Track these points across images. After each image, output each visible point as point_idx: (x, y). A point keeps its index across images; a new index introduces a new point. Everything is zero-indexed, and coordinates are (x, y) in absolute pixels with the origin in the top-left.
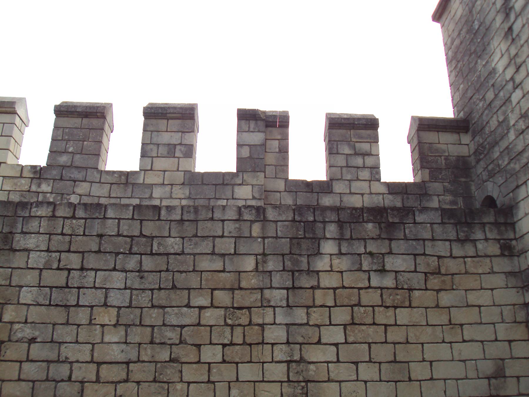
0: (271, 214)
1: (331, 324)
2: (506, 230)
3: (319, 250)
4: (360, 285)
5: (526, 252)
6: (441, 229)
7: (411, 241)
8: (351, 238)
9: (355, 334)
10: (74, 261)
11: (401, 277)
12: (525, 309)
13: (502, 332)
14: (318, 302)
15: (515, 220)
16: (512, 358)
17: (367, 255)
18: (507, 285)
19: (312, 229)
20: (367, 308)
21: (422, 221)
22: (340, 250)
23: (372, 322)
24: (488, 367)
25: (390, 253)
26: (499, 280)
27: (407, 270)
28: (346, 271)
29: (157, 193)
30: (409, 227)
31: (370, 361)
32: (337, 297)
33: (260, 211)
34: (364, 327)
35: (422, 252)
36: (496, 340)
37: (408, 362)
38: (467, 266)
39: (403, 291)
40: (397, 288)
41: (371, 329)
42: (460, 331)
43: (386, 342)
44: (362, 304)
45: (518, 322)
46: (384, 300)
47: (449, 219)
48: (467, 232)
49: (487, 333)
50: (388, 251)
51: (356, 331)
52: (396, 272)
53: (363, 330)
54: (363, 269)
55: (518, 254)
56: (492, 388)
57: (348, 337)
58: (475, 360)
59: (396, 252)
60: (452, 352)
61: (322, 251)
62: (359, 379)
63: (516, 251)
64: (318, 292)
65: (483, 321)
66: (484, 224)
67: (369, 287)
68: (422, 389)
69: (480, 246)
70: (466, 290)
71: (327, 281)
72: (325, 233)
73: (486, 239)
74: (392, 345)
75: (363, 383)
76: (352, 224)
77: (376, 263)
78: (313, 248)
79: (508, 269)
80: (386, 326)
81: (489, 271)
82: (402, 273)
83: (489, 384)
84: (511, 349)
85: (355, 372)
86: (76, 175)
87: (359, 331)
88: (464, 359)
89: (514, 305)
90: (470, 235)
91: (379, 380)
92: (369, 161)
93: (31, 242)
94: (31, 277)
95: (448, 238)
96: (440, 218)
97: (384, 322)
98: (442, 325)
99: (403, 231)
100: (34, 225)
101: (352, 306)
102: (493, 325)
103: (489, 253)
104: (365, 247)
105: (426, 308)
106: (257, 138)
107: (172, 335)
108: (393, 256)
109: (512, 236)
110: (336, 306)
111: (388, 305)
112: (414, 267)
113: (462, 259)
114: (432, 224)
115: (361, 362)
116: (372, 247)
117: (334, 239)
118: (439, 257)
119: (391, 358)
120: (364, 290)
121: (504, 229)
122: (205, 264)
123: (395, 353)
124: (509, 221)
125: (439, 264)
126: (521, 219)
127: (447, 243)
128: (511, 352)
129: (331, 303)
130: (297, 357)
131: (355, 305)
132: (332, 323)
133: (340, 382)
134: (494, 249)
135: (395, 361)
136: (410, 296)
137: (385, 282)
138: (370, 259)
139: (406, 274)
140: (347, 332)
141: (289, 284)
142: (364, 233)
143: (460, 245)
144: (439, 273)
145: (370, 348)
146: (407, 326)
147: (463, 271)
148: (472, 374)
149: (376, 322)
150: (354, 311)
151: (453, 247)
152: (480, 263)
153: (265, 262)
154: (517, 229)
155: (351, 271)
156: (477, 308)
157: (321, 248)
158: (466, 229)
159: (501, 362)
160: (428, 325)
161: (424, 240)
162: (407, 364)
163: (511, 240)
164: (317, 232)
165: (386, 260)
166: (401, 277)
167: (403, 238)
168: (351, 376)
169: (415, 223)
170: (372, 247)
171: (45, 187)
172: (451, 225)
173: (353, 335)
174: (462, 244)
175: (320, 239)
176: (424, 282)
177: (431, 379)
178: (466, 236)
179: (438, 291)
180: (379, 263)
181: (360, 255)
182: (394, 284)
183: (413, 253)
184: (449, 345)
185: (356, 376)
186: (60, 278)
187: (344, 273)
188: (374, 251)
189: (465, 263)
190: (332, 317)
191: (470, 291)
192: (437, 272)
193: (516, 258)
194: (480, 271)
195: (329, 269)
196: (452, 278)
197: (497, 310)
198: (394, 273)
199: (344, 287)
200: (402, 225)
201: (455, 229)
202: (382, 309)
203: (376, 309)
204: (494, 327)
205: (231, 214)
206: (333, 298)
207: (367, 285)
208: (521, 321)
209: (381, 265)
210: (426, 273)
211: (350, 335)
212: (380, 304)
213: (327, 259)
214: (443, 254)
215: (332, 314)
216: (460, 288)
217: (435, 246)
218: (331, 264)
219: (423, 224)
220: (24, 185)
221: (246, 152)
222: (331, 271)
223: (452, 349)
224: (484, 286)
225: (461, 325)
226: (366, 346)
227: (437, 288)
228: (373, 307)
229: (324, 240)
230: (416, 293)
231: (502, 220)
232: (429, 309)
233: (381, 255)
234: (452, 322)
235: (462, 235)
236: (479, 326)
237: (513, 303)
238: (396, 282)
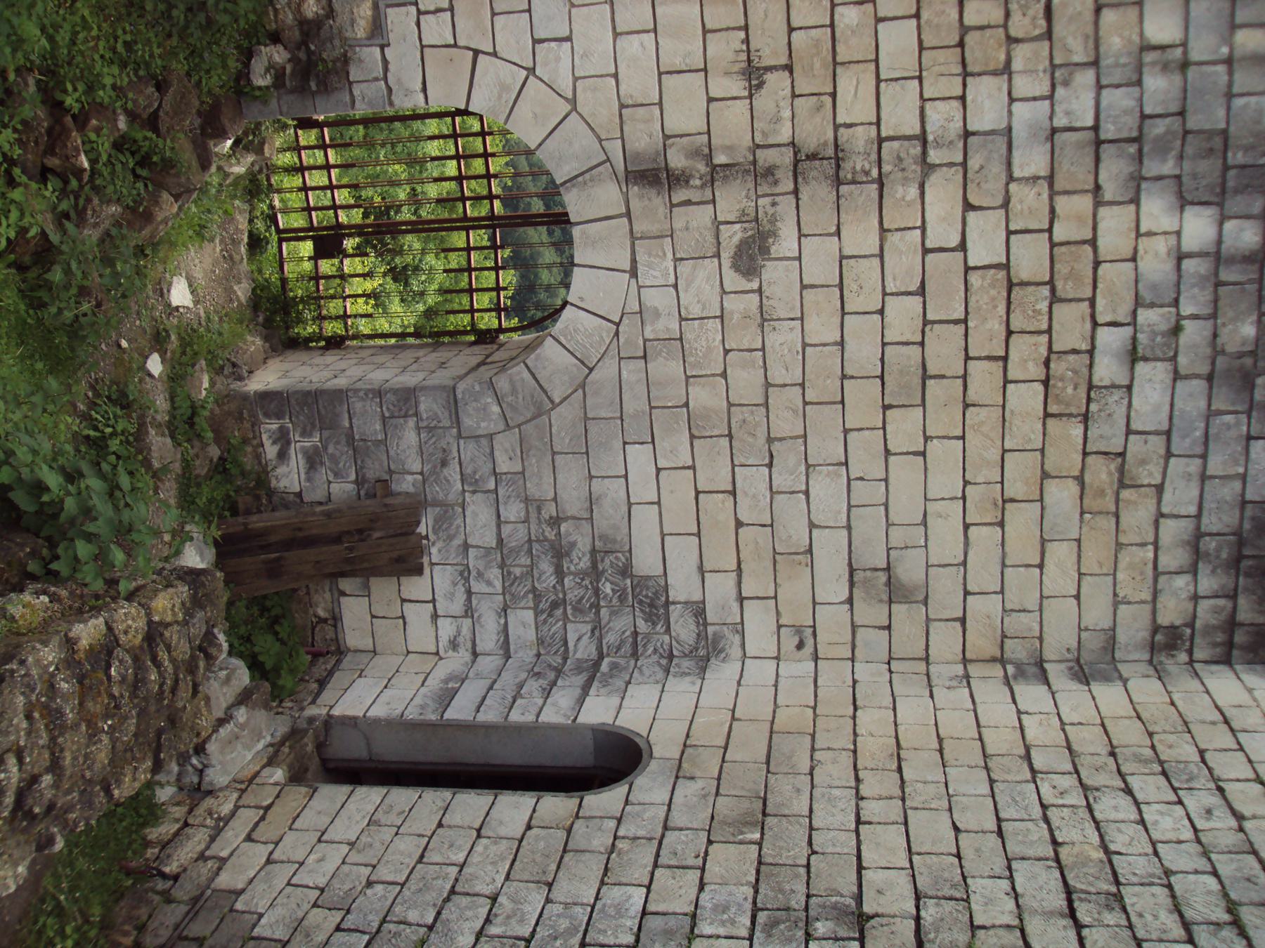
1: (1009, 233)
2: (1215, 645)
3: (1192, 203)
4: (1100, 303)
5: (1160, 678)
6: (1228, 498)
7: (1202, 425)
8: (1218, 284)
9: (987, 290)
11: (1116, 398)
12: (1032, 661)
13: (984, 609)
14: (1062, 203)
15: (1238, 667)
16: (928, 619)
17: (1173, 320)
18: (1087, 629)
19: (1247, 186)
20: (1046, 317)
21: (1253, 455)
22: (1190, 255)
23: (1012, 328)
24: (910, 570)
25: (1177, 376)
26: (1097, 613)
27: (1132, 414)
28: (1136, 269)
30: (1238, 424)
31: (926, 323)
32: (1073, 248)
34: (1002, 309)
35: (1174, 450)
36: (967, 593)
37: (923, 404)
38: (1134, 548)
39: (1084, 401)
40: (1091, 387)
41: (997, 326)
42: (988, 521)
43: (968, 358)
44: (1055, 306)
45: (1002, 642)
46: (1064, 357)
47: (1253, 519)
48: (1218, 557)
49: (983, 574)
50: (1182, 371)
51: (993, 292)
52: (1129, 388)
53: (995, 307)
54: (1140, 311)
55: (1155, 662)
56: (868, 573)
57: (980, 272)
58: (926, 546)
59: (1177, 391)
60: (943, 499)
61: (1190, 212)
62: (887, 298)
63: (1163, 659)
64: (1086, 202)
65: (1008, 571)
66: (1233, 596)
67: (1095, 324)
68: (867, 433)
69: (1181, 582)
70: (1079, 541)
71: (1114, 224)
72: (1236, 217)
73: (1195, 598)
74: (961, 372)
75: (879, 307)
76: (1256, 286)
77: (1153, 340)
78: (1197, 189)
79: (1122, 637)
80: (1005, 359)
81: (1121, 595)
82: (1125, 402)
83: (876, 570)
84: (947, 620)
85: (903, 290)
87: (993, 299)
88: (929, 525)
89: (1041, 639)
90: (1210, 562)
91: (886, 340)
95: (1205, 513)
96: (1258, 499)
97: (1014, 356)
98: (1002, 483)
99: (1231, 408)
101: (1051, 283)
102: (998, 589)
103: (1161, 599)
104: (1195, 317)
105: (1042, 451)
108: (1169, 382)
109: (1198, 654)
110: (1053, 245)
111: (1052, 365)
112: (1140, 429)
113: (1151, 539)
114: (1243, 478)
115: (924, 303)
116: (1193, 333)
117: (1219, 242)
118: (1160, 489)
119: (932, 370)
120: (1088, 311)
121: (1218, 640)
123: (943, 377)
124: (1235, 653)
125: (1143, 486)
126: (1239, 678)
127: (1193, 510)
128: (940, 620)
129: (1060, 233)
130: (934, 156)
131: (1053, 291)
132: (1013, 237)
133: (881, 256)
134: (1171, 612)
135: (925, 377)
136: (1070, 415)
137: (1106, 360)
138: (1164, 327)
139: (1124, 409)
140: (992, 271)
141: (1108, 131)
142: (1230, 314)
143: (1186, 537)
144: (1122, 485)
145: (956, 322)
146: (1004, 407)
147: (1122, 539)
148: (897, 536)
149: (1014, 338)
150: (1040, 288)
151: (1183, 523)
152: (1138, 578)
153: (1165, 67)
154: (1214, 668)
155: (1137, 282)
156: (1037, 561)
157: (1197, 208)
158: (1224, 555)
159: (921, 597)
160: (1004, 451)
161: (1204, 457)
162: (919, 402)
163: (1190, 652)
164: (1239, 198)
165: (1159, 364)
166: (1116, 398)
167: (1213, 408)
168: (894, 279)
169: (1249, 438)
170: (1193, 333)
172: (1236, 521)
173: (986, 285)
174: (1188, 543)
175: (1220, 205)
176: (1103, 450)
177: (887, 452)
178: (1207, 554)
179: (1080, 480)
180: (1153, 349)
181: (1176, 303)
182: (1101, 380)
183: (1174, 429)
184: (960, 495)
185: (894, 290)
187: (1130, 265)
188: (1184, 339)
189: (1143, 545)
190: (1027, 236)
191: (1076, 549)
193: (1147, 656)
194: (1120, 576)
195: (1143, 229)
196: (1108, 513)
197: (1032, 602)
198: (1126, 382)
199: (1097, 264)
200: (1244, 407)
201: (1226, 530)
202: (1043, 351)
203: (1044, 339)
204: (995, 593)
206: (1073, 239)
207: (1100, 320)
208: (1006, 647)
209: (1148, 354)
210: (1122, 455)
211: (983, 278)
212: (1056, 348)
213: (1167, 222)
214: (1167, 496)
215: (1035, 235)
216: (1085, 529)
217: (1189, 480)
218: (1156, 234)
219: (1243, 458)
222: (1138, 235)
223: (951, 499)
224: (1087, 581)
225: (1001, 524)
226: (960, 314)
227: (1087, 478)
228: (1049, 331)
229: (1218, 217)
230: (1078, 431)
231: (1239, 637)
232: (1039, 457)
233: (1172, 354)
234: (1008, 505)
235: (1210, 544)
236: (999, 561)
237: (1045, 636)
238: (1105, 387)
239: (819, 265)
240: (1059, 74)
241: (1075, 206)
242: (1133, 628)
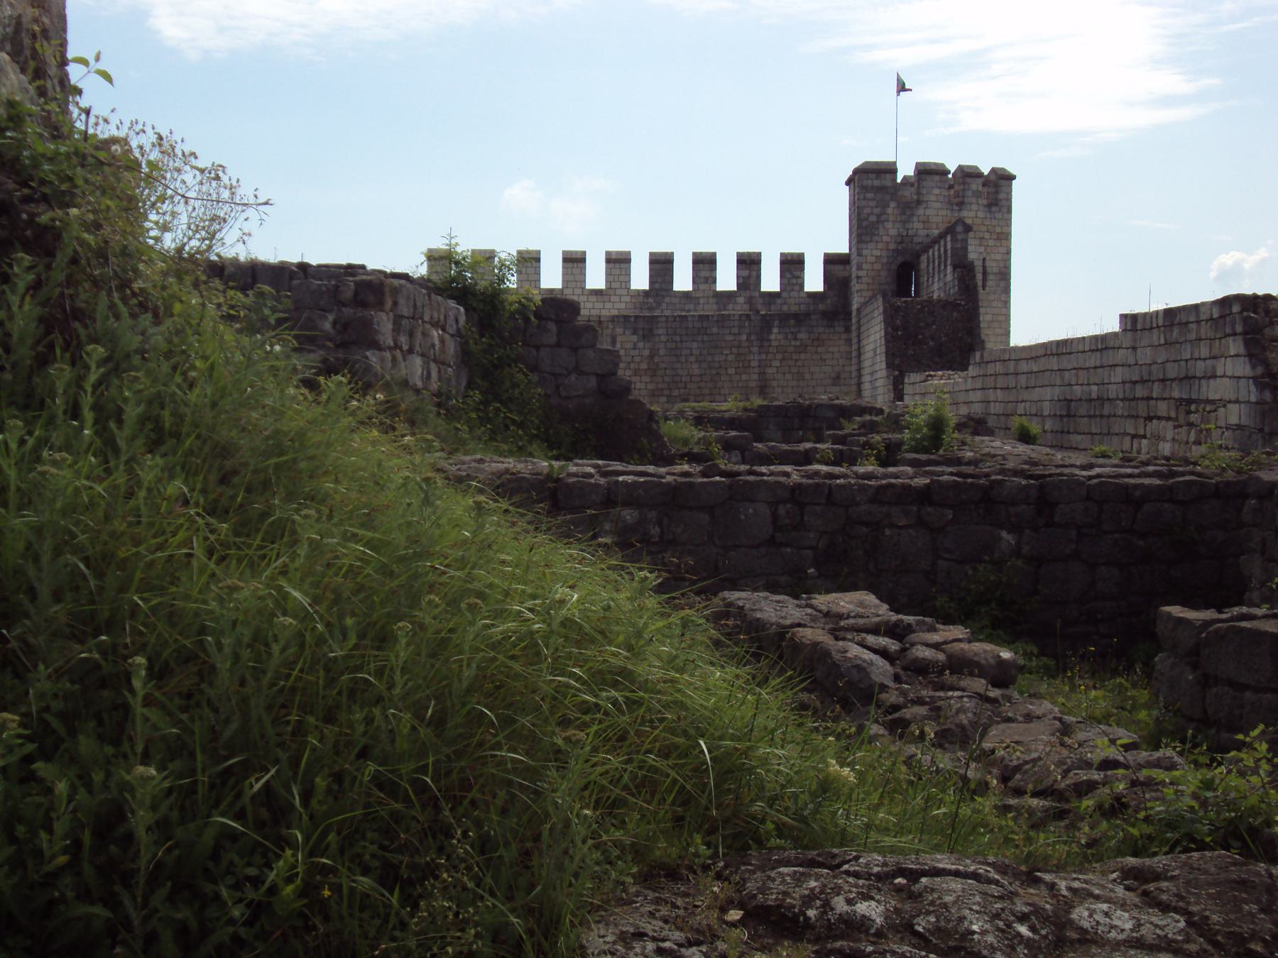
0: (753, 318)
10: (678, 338)
26: (842, 342)
29: (701, 301)
33: (748, 316)
71: (774, 343)
86: (665, 293)
92: (799, 281)
93: (660, 331)
94: (662, 345)
100: (660, 325)
106: (745, 273)
107: (716, 365)
122: (728, 338)
134: (842, 329)
171: (651, 300)
186: (673, 345)
192: (818, 339)
205: (737, 318)
220: (641, 299)
221: (741, 281)
239: (779, 390)
240: (750, 352)
241: (771, 350)
242: (844, 336)
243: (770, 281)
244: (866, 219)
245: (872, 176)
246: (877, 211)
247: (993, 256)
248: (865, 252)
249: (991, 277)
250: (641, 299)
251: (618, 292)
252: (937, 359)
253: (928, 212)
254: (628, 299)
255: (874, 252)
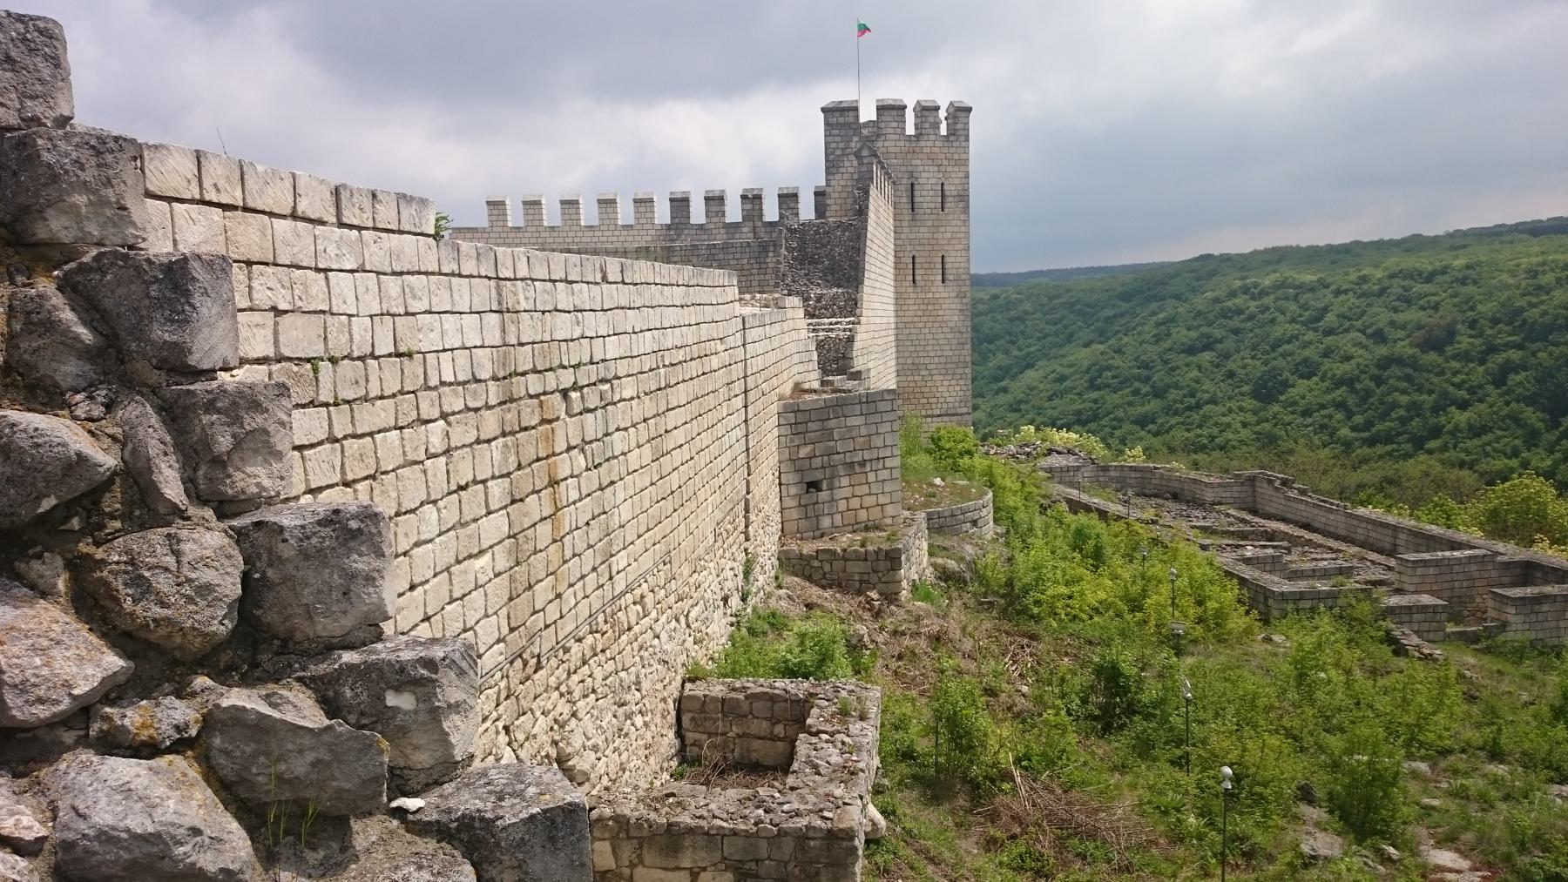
106: (749, 206)
220: (664, 232)
243: (771, 212)
244: (833, 153)
245: (838, 114)
246: (841, 145)
247: (951, 181)
248: (833, 183)
249: (950, 199)
250: (664, 232)
251: (645, 227)
252: (830, 278)
253: (886, 144)
254: (653, 232)
255: (840, 181)
